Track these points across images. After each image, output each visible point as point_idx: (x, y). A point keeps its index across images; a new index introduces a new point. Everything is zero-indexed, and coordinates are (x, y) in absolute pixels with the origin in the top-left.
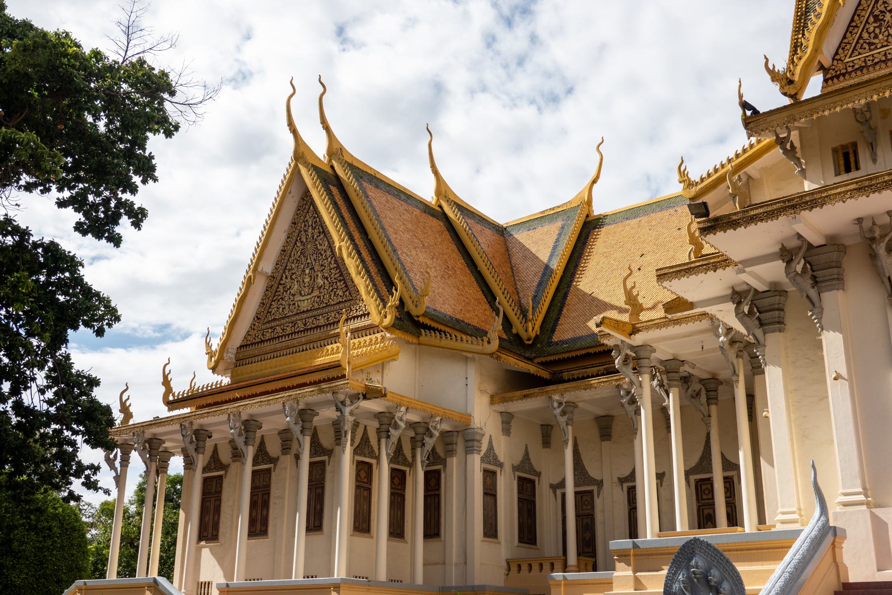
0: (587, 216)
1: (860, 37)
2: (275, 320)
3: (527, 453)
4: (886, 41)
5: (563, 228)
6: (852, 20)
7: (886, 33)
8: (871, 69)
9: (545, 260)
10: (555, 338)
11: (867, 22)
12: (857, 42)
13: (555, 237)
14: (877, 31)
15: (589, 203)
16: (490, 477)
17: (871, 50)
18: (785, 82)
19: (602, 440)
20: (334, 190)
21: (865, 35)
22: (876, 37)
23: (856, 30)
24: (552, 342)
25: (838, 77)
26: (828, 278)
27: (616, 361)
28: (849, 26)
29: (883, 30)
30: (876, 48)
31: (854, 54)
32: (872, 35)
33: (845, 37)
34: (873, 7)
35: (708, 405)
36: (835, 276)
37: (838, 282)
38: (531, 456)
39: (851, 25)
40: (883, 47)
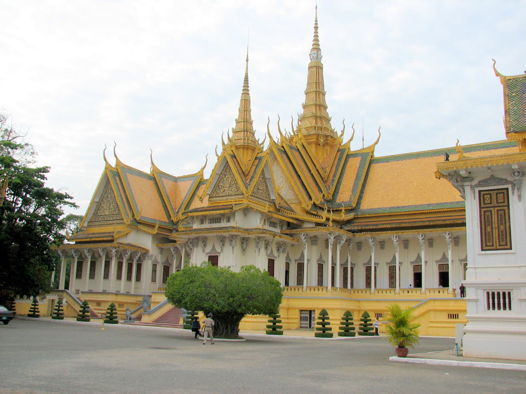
0: (201, 179)
2: (98, 216)
3: (167, 259)
5: (193, 183)
15: (203, 175)
16: (155, 266)
20: (117, 178)
37: (197, 246)
38: (169, 259)
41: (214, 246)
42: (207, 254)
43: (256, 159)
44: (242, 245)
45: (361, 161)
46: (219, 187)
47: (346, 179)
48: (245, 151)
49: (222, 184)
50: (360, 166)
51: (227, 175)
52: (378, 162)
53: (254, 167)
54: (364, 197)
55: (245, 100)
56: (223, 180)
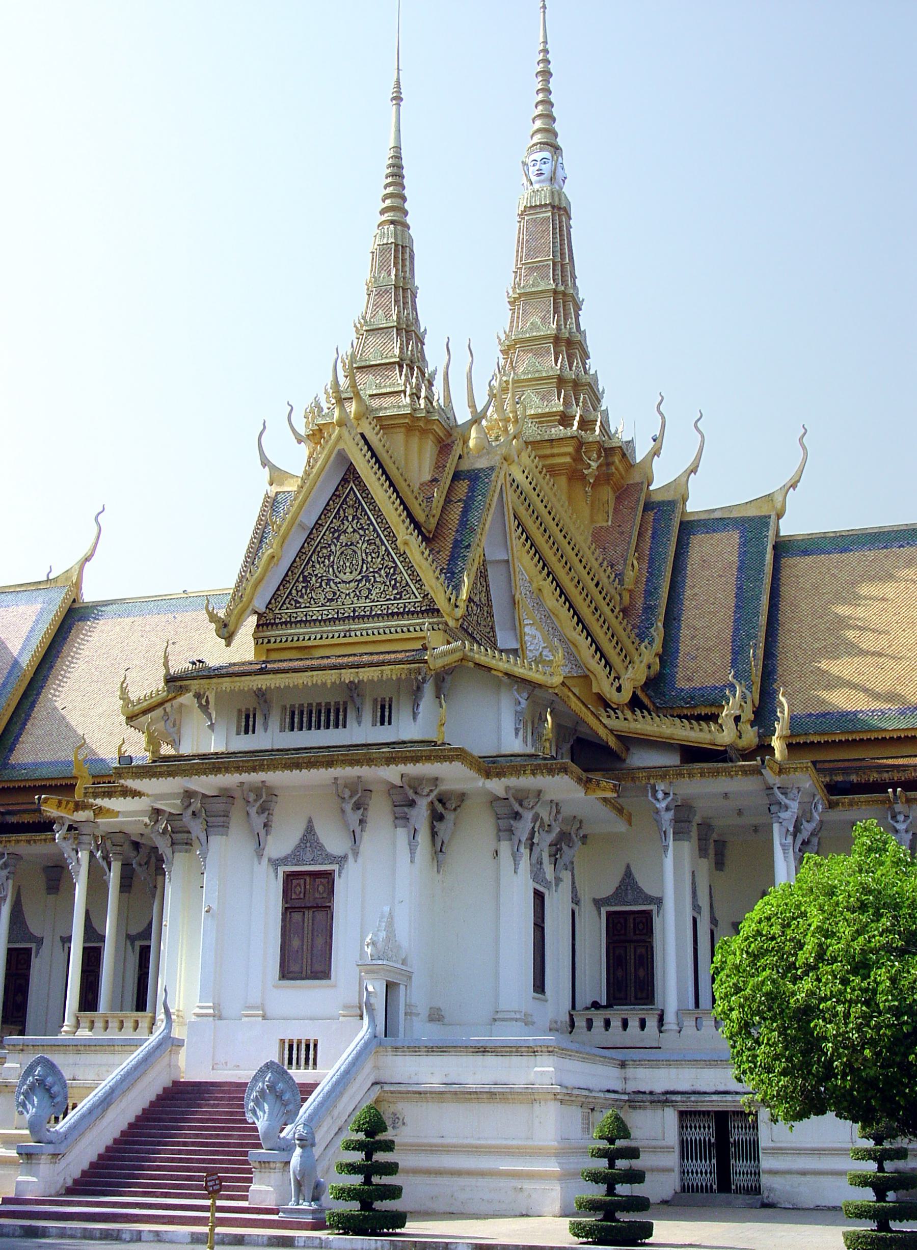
0: (74, 601)
1: (290, 593)
4: (310, 602)
6: (287, 575)
7: (310, 595)
8: (293, 625)
9: (15, 654)
10: (13, 760)
11: (297, 580)
12: (287, 597)
13: (30, 624)
14: (304, 591)
15: (78, 585)
17: (296, 608)
18: (221, 623)
19: (49, 894)
21: (294, 592)
22: (302, 596)
23: (288, 585)
24: (8, 763)
25: (267, 625)
26: (216, 824)
27: (57, 835)
28: (283, 579)
29: (308, 591)
30: (300, 607)
31: (285, 607)
32: (299, 594)
33: (278, 589)
34: (304, 568)
35: (156, 875)
36: (222, 824)
37: (224, 828)
39: (284, 581)
40: (305, 607)
41: (310, 830)
42: (275, 863)
43: (457, 476)
44: (432, 828)
45: (743, 544)
46: (305, 580)
47: (696, 607)
48: (415, 441)
49: (319, 570)
50: (741, 561)
51: (345, 532)
52: (805, 553)
53: (456, 511)
54: (780, 670)
55: (396, 245)
56: (325, 551)
